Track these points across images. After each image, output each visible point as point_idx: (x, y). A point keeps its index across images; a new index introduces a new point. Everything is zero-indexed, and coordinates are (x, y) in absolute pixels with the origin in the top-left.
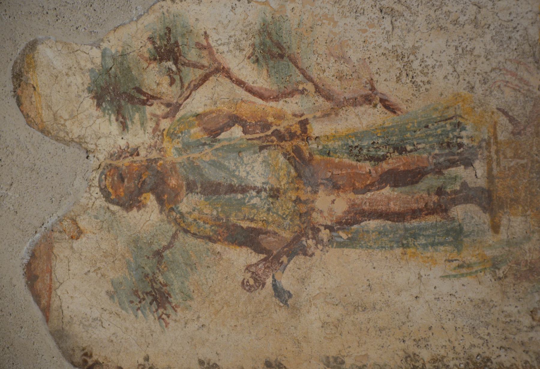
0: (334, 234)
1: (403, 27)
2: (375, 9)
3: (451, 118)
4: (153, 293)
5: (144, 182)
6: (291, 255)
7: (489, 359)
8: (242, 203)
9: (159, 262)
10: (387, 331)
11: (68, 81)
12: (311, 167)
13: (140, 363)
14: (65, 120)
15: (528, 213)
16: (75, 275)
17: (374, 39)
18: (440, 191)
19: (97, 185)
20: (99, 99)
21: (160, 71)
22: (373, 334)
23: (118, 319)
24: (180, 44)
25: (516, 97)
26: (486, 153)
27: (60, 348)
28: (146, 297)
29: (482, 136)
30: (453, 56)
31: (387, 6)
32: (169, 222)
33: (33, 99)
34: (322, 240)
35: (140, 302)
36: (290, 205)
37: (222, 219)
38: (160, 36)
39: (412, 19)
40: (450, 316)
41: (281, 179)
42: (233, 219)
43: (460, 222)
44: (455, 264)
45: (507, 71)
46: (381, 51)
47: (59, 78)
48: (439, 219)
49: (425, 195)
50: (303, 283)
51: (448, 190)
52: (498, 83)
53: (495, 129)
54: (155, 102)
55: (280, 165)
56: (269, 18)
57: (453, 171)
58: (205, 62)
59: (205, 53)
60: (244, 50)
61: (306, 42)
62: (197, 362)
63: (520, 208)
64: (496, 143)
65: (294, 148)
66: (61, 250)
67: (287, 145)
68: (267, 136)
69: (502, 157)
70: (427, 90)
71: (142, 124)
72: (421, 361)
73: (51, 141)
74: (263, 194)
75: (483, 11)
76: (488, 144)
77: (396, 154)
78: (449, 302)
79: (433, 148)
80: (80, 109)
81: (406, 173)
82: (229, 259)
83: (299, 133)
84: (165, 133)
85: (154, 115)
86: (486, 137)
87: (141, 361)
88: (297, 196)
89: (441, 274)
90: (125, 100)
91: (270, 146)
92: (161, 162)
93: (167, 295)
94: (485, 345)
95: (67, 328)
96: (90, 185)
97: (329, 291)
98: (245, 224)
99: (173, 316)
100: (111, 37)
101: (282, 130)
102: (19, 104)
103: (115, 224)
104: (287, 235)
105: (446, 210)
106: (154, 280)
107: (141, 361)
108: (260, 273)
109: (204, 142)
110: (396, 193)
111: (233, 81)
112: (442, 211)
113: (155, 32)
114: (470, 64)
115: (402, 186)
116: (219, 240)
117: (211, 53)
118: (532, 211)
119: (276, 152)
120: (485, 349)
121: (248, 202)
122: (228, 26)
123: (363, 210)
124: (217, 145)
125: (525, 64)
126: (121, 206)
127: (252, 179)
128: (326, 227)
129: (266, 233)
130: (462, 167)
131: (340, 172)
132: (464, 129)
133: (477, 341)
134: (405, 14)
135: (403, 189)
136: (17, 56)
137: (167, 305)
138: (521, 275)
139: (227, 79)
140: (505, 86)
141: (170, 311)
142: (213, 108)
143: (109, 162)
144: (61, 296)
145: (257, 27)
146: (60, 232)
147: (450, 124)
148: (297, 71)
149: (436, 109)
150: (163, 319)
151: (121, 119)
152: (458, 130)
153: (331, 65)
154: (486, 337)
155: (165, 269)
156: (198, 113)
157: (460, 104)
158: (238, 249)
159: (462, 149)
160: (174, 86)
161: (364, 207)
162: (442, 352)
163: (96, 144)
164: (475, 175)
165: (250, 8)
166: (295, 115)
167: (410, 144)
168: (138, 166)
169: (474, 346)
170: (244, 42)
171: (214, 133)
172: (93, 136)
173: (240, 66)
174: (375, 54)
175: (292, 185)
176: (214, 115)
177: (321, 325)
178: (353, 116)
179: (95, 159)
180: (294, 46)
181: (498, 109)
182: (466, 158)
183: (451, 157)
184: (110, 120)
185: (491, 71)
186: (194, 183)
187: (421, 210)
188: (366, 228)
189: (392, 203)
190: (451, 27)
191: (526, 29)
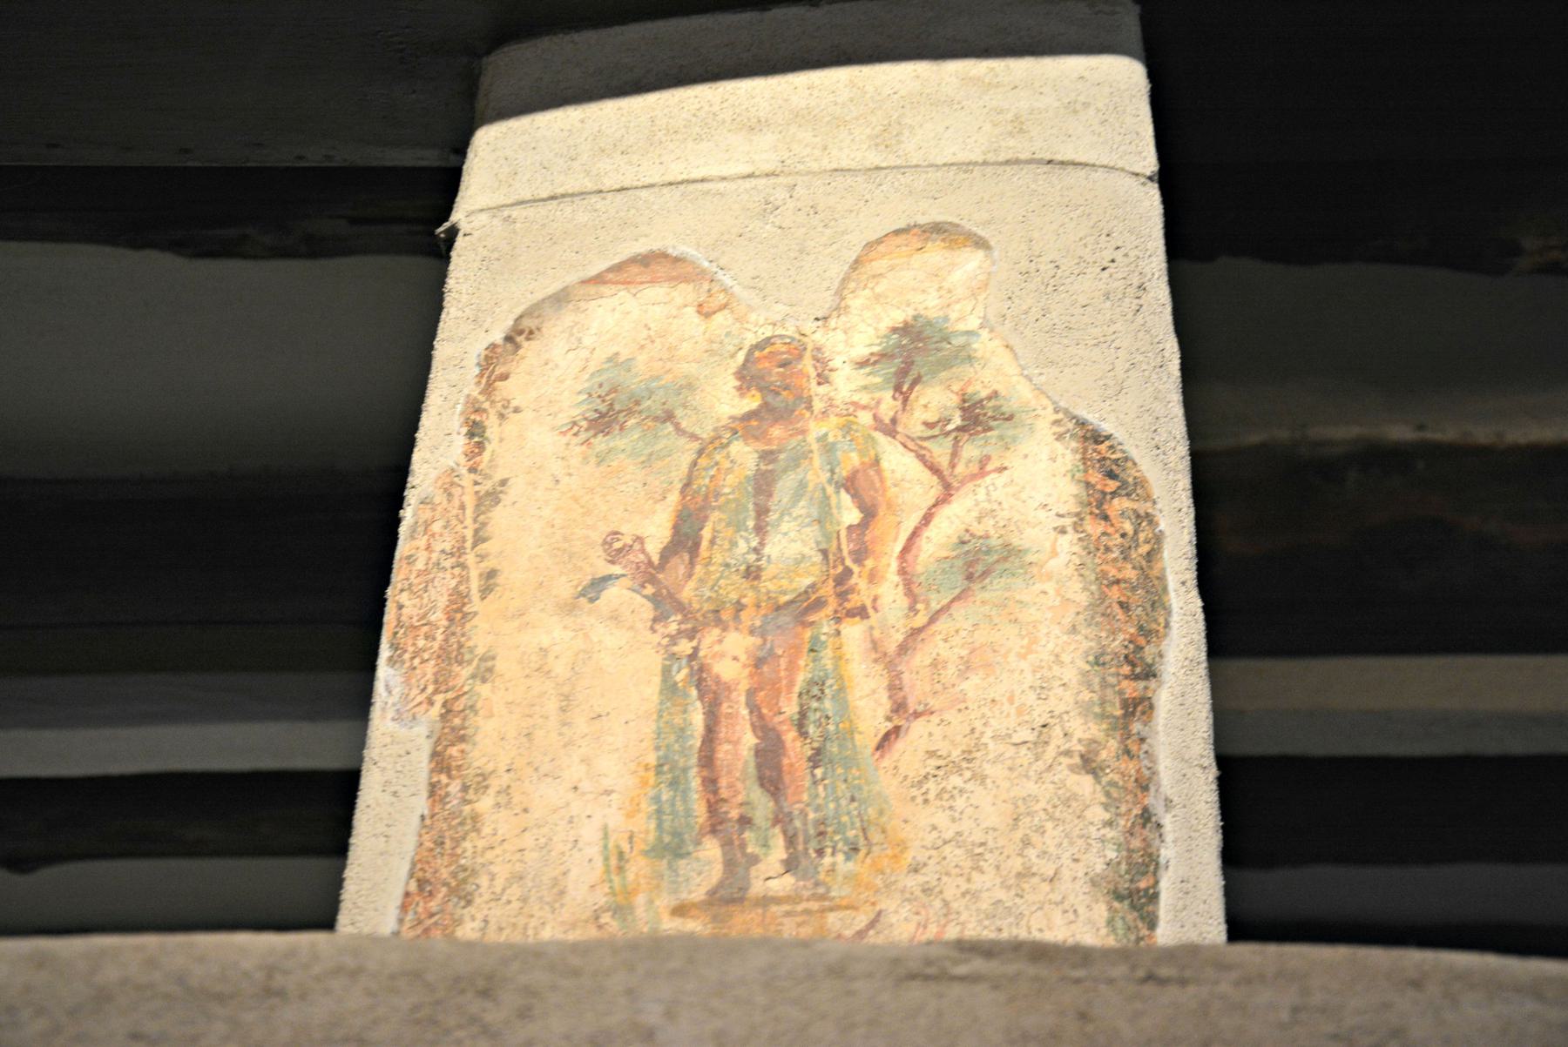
0: (684, 662)
6: (655, 599)
7: (469, 903)
8: (739, 526)
9: (656, 419)
18: (745, 821)
20: (905, 330)
21: (946, 408)
26: (806, 894)
32: (715, 429)
36: (734, 596)
39: (1031, 773)
40: (543, 840)
42: (715, 516)
48: (701, 820)
49: (740, 798)
51: (747, 835)
53: (847, 908)
54: (899, 403)
56: (1029, 558)
57: (778, 842)
58: (960, 469)
59: (974, 468)
64: (823, 911)
66: (685, 293)
68: (843, 560)
69: (799, 919)
70: (913, 798)
71: (865, 388)
74: (752, 557)
75: (1046, 887)
76: (823, 897)
77: (810, 753)
79: (818, 809)
81: (778, 768)
83: (848, 605)
85: (879, 403)
86: (833, 894)
87: (514, 403)
89: (611, 825)
98: (706, 533)
100: (997, 342)
102: (897, 232)
104: (687, 593)
105: (714, 831)
106: (630, 412)
107: (514, 403)
108: (631, 557)
110: (745, 753)
117: (973, 477)
120: (486, 897)
124: (830, 490)
128: (696, 649)
129: (692, 564)
130: (785, 856)
132: (848, 859)
133: (499, 884)
135: (752, 764)
137: (591, 433)
141: (583, 436)
142: (889, 483)
143: (810, 347)
145: (1016, 541)
148: (945, 601)
149: (881, 813)
151: (873, 359)
154: (504, 898)
157: (889, 852)
158: (670, 525)
161: (725, 705)
162: (486, 830)
164: (770, 875)
166: (875, 599)
167: (825, 773)
169: (492, 880)
170: (992, 522)
171: (850, 484)
180: (986, 595)
181: (879, 913)
187: (715, 792)
188: (690, 708)
190: (1019, 835)
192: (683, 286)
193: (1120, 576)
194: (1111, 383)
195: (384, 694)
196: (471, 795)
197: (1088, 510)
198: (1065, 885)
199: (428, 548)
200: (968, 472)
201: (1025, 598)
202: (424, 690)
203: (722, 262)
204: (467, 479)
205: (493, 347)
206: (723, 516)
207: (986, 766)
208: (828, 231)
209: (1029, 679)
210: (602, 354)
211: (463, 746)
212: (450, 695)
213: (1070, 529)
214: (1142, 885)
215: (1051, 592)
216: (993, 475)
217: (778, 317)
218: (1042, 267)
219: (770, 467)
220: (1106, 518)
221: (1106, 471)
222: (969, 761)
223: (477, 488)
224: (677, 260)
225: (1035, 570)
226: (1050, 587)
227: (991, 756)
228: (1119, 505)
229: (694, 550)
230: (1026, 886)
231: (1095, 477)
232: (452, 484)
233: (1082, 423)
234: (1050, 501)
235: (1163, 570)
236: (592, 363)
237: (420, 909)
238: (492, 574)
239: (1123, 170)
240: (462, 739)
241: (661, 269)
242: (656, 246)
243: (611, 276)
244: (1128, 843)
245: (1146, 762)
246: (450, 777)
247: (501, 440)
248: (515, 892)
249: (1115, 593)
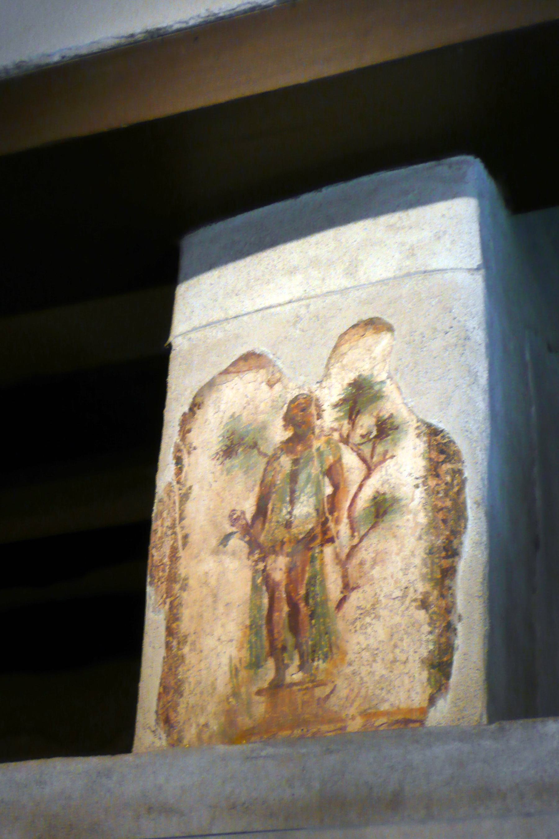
0: (261, 573)
6: (249, 543)
8: (283, 501)
11: (367, 359)
18: (284, 649)
26: (307, 680)
32: (275, 450)
36: (280, 538)
40: (208, 665)
42: (274, 496)
49: (282, 638)
51: (285, 655)
54: (350, 426)
57: (297, 657)
58: (375, 459)
66: (262, 375)
69: (304, 692)
74: (288, 517)
75: (402, 667)
76: (312, 681)
84: (330, 437)
85: (342, 426)
86: (318, 679)
98: (270, 506)
100: (393, 386)
102: (354, 326)
104: (262, 539)
106: (239, 444)
108: (240, 522)
120: (188, 693)
124: (321, 477)
128: (265, 566)
129: (264, 523)
132: (324, 662)
135: (287, 621)
141: (221, 460)
143: (314, 399)
145: (397, 495)
146: (273, 372)
148: (367, 530)
151: (341, 402)
161: (277, 593)
163: (324, 388)
166: (338, 532)
190: (392, 643)
193: (443, 506)
196: (181, 647)
197: (430, 473)
202: (162, 597)
205: (184, 414)
207: (381, 611)
208: (323, 330)
209: (400, 565)
210: (228, 414)
212: (172, 599)
213: (421, 485)
214: (445, 659)
215: (411, 519)
219: (297, 467)
220: (438, 476)
221: (440, 449)
224: (259, 356)
225: (404, 509)
226: (410, 517)
227: (383, 606)
228: (447, 467)
230: (394, 667)
231: (434, 455)
233: (429, 426)
234: (413, 471)
235: (465, 498)
238: (186, 537)
239: (461, 269)
241: (252, 362)
243: (232, 369)
244: (439, 640)
248: (198, 691)
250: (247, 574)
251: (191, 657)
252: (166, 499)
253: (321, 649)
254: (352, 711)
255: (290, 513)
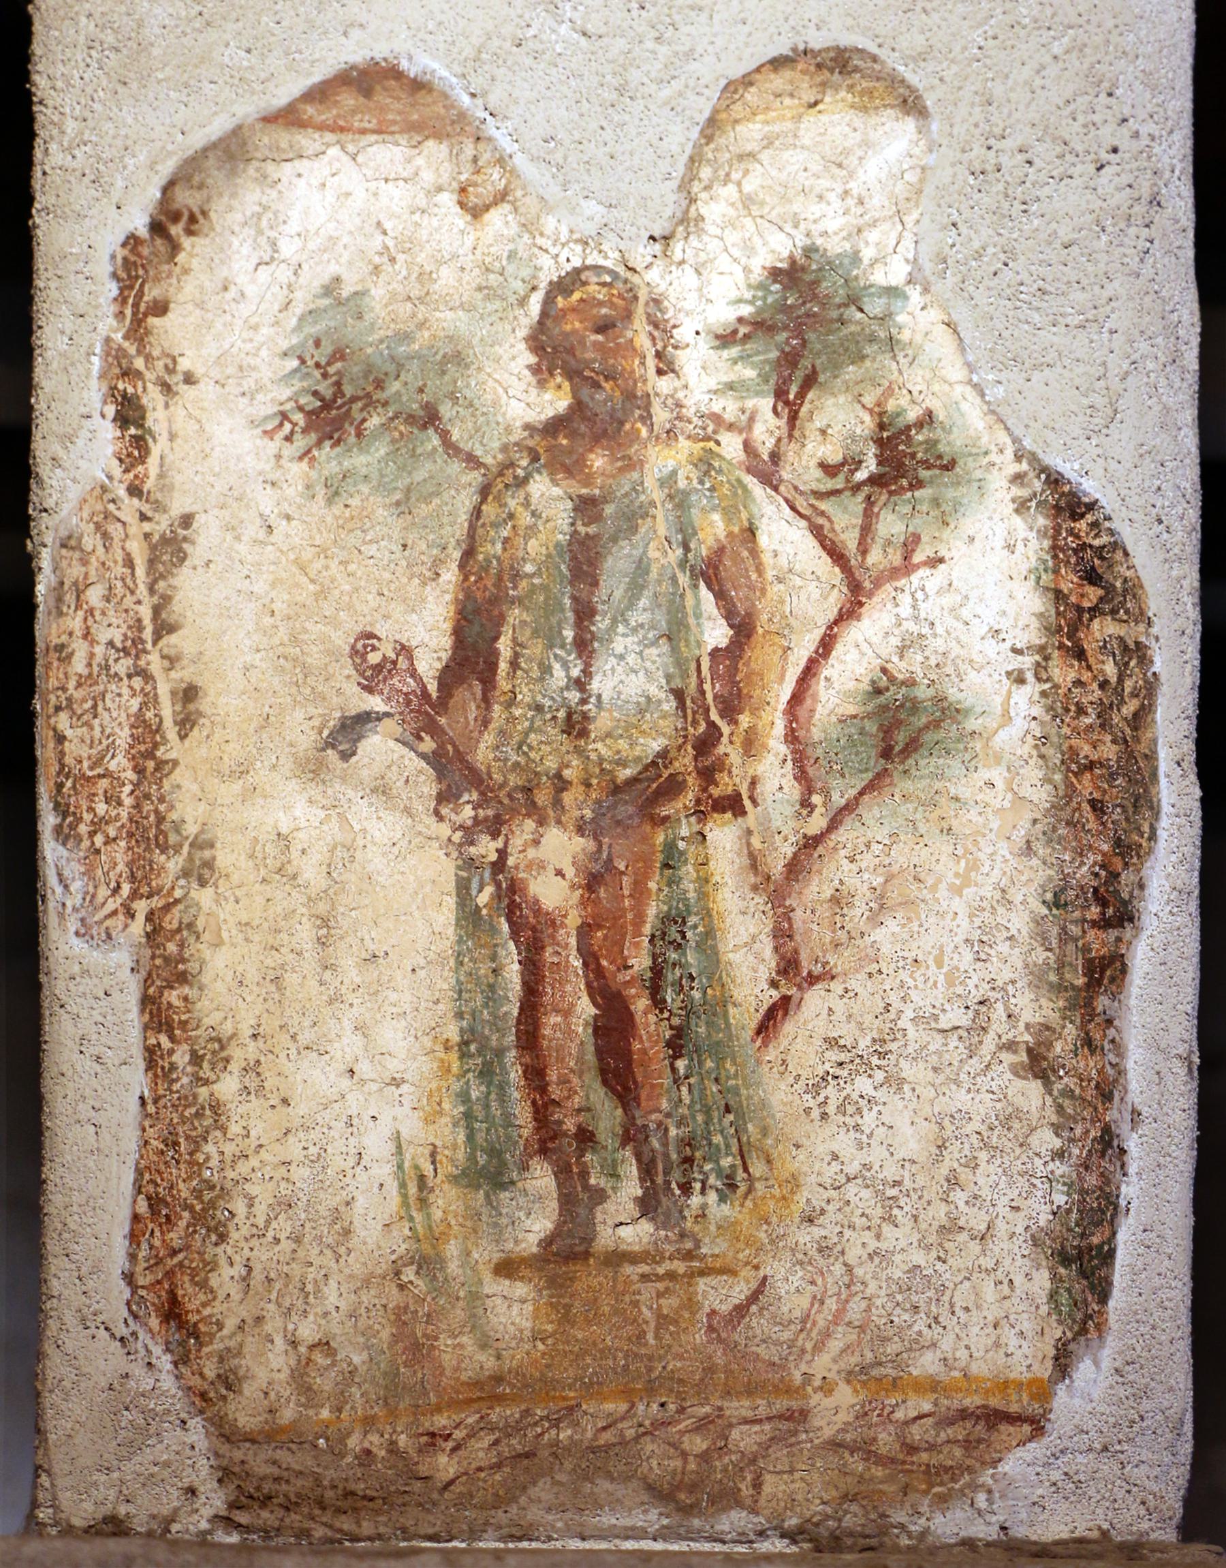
1: (947, 1056)
2: (988, 987)
3: (746, 1170)
4: (339, 401)
5: (597, 386)
6: (437, 761)
8: (553, 640)
9: (411, 419)
10: (277, 996)
11: (832, 197)
12: (637, 820)
13: (180, 360)
14: (739, 184)
15: (541, 1346)
16: (375, 194)
17: (921, 986)
18: (585, 1137)
19: (588, 262)
20: (790, 275)
21: (853, 438)
22: (269, 962)
23: (276, 307)
24: (917, 494)
25: (791, 1322)
26: (669, 1249)
27: (205, 150)
28: (330, 381)
29: (707, 1240)
30: (880, 1176)
31: (994, 1017)
32: (505, 448)
33: (787, 101)
34: (472, 843)
35: (318, 365)
36: (551, 764)
37: (515, 588)
38: (936, 442)
39: (963, 1076)
40: (313, 1150)
41: (608, 741)
42: (515, 615)
43: (520, 1185)
44: (428, 1169)
45: (847, 1301)
46: (896, 1004)
47: (836, 171)
48: (526, 1133)
50: (374, 791)
51: (588, 1157)
52: (819, 1282)
55: (641, 741)
56: (972, 724)
57: (631, 1170)
58: (875, 557)
59: (896, 558)
60: (901, 657)
61: (919, 816)
62: (187, 510)
63: (549, 1328)
64: (692, 1275)
65: (680, 778)
67: (686, 761)
68: (708, 710)
69: (660, 1286)
70: (808, 1111)
71: (730, 386)
72: (213, 1077)
73: (691, 144)
74: (574, 696)
75: (975, 1247)
76: (689, 1256)
77: (668, 1034)
78: (344, 1149)
80: (767, 225)
82: (424, 600)
83: (716, 792)
84: (712, 444)
85: (752, 419)
86: (704, 1251)
87: (184, 364)
88: (570, 783)
89: (405, 1134)
90: (787, 342)
91: (685, 717)
92: (644, 432)
93: (336, 436)
94: (254, 1231)
95: (251, 171)
96: (586, 243)
97: (358, 854)
98: (504, 646)
99: (289, 450)
100: (934, 314)
101: (721, 749)
103: (497, 304)
104: (483, 753)
105: (544, 1151)
106: (370, 403)
108: (395, 681)
109: (692, 546)
110: (581, 1029)
111: (830, 628)
112: (542, 1142)
113: (943, 429)
114: (863, 1215)
115: (596, 1044)
116: (466, 578)
117: (895, 573)
118: (544, 1354)
119: (670, 731)
121: (556, 656)
122: (957, 618)
123: (543, 948)
124: (684, 579)
125: (859, 1344)
126: (540, 323)
127: (608, 667)
128: (503, 854)
129: (487, 701)
130: (640, 1192)
131: (626, 892)
132: (722, 1199)
133: (261, 1211)
134: (975, 1059)
135: (590, 1049)
136: (890, 63)
137: (313, 437)
138: (405, 1323)
139: (836, 611)
140: (814, 1297)
141: (301, 443)
142: (770, 574)
143: (643, 295)
144: (325, 158)
145: (953, 694)
147: (733, 1166)
148: (853, 792)
149: (765, 1132)
150: (281, 425)
151: (743, 330)
152: (719, 1184)
153: (866, 876)
154: (270, 1234)
155: (396, 434)
156: (758, 533)
157: (776, 1191)
158: (448, 626)
159: (678, 1192)
160: (819, 473)
161: (549, 950)
162: (234, 1129)
163: (682, 262)
164: (622, 1225)
165: (996, 677)
166: (753, 783)
167: (688, 1067)
168: (633, 371)
170: (919, 658)
171: (710, 573)
172: (703, 256)
173: (864, 647)
174: (888, 988)
175: (597, 770)
176: (754, 576)
177: (284, 831)
178: (752, 930)
179: (649, 259)
180: (907, 785)
181: (765, 1278)
182: (659, 1202)
183: (660, 1167)
184: (740, 301)
185: (845, 1265)
186: (597, 518)
187: (543, 1089)
189: (559, 1019)
190: (944, 1171)
191: (934, 1345)
192: (431, 143)
194: (1099, 401)
195: (59, 890)
196: (206, 1072)
198: (1000, 1245)
199: (87, 635)
200: (885, 564)
201: (964, 792)
203: (493, 100)
204: (129, 507)
206: (525, 616)
209: (964, 926)
211: (186, 990)
213: (1029, 676)
215: (1000, 785)
216: (924, 572)
217: (590, 229)
218: (1004, 160)
220: (1080, 654)
222: (882, 1055)
223: (147, 527)
225: (978, 745)
226: (997, 775)
229: (488, 680)
230: (947, 1245)
231: (1069, 582)
232: (107, 515)
233: (1054, 480)
234: (1004, 624)
236: (298, 295)
237: (157, 1242)
238: (189, 694)
240: (183, 978)
242: (381, 51)
245: (1111, 1057)
246: (172, 1039)
247: (172, 437)
248: (283, 1226)
249: (1086, 786)
250: (441, 869)
251: (249, 1118)
252: (91, 541)
253: (713, 1155)
254: (822, 1366)
255: (580, 684)
